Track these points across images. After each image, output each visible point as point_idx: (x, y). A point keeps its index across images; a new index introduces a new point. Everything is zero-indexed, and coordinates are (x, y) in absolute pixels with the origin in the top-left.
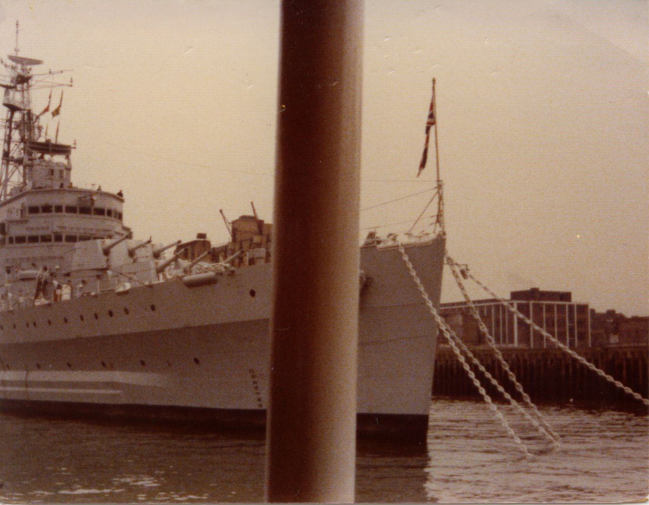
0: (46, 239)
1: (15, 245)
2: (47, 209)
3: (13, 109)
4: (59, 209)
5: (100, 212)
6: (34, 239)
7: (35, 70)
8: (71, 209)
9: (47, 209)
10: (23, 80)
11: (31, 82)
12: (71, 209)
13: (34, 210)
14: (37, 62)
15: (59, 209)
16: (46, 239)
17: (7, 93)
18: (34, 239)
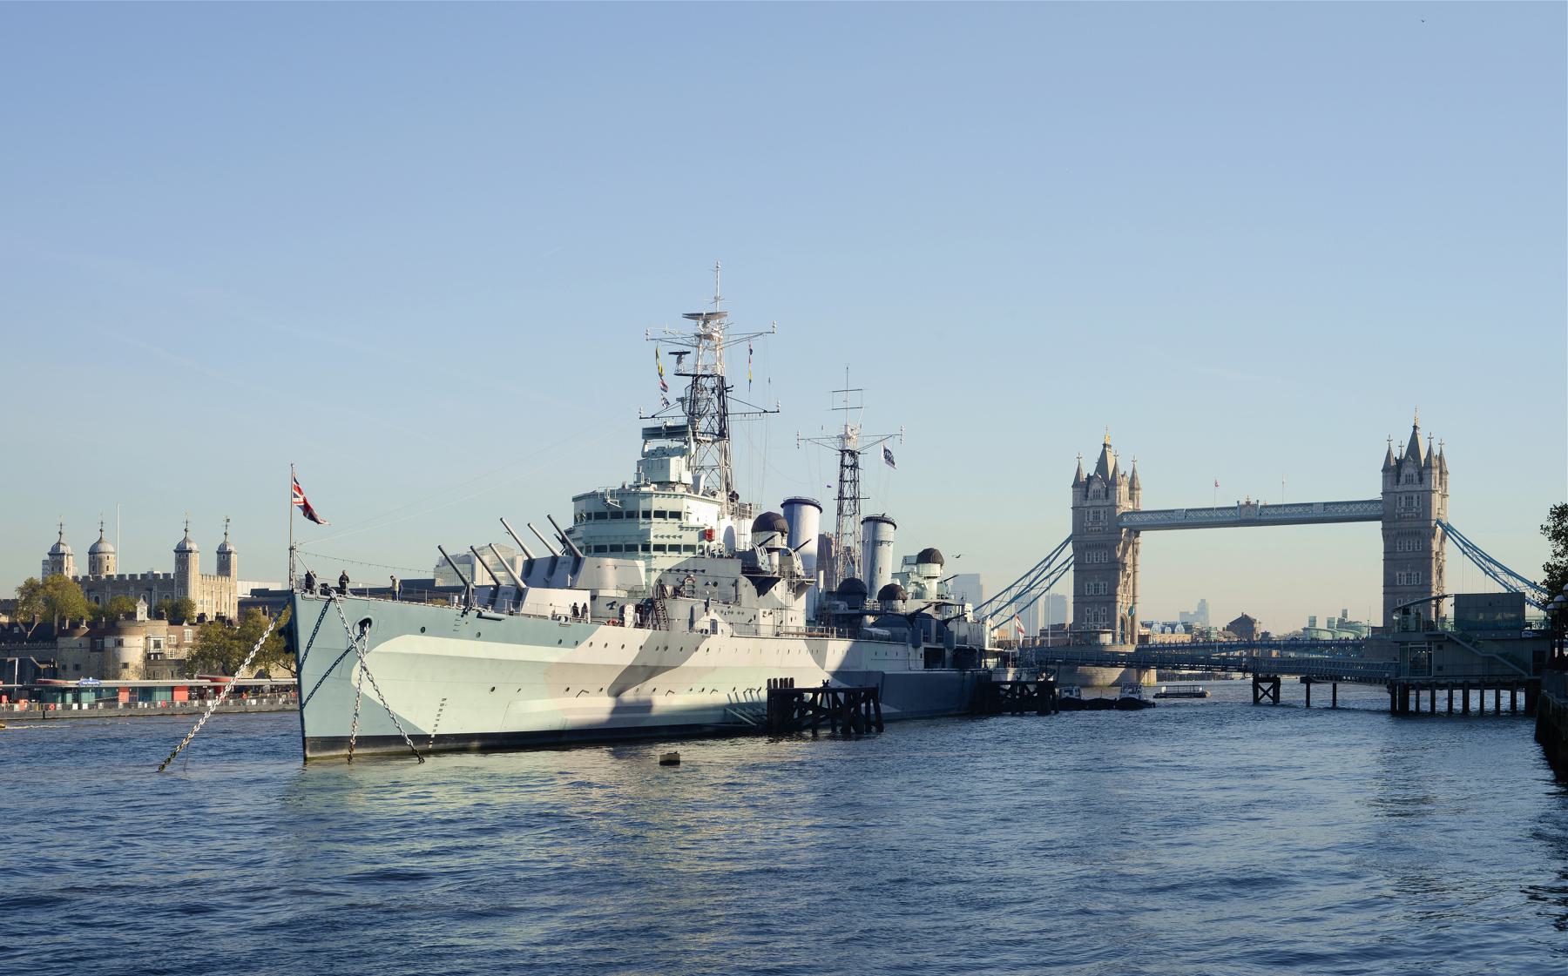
3: (696, 377)
5: (632, 515)
8: (600, 516)
12: (600, 516)
17: (679, 361)
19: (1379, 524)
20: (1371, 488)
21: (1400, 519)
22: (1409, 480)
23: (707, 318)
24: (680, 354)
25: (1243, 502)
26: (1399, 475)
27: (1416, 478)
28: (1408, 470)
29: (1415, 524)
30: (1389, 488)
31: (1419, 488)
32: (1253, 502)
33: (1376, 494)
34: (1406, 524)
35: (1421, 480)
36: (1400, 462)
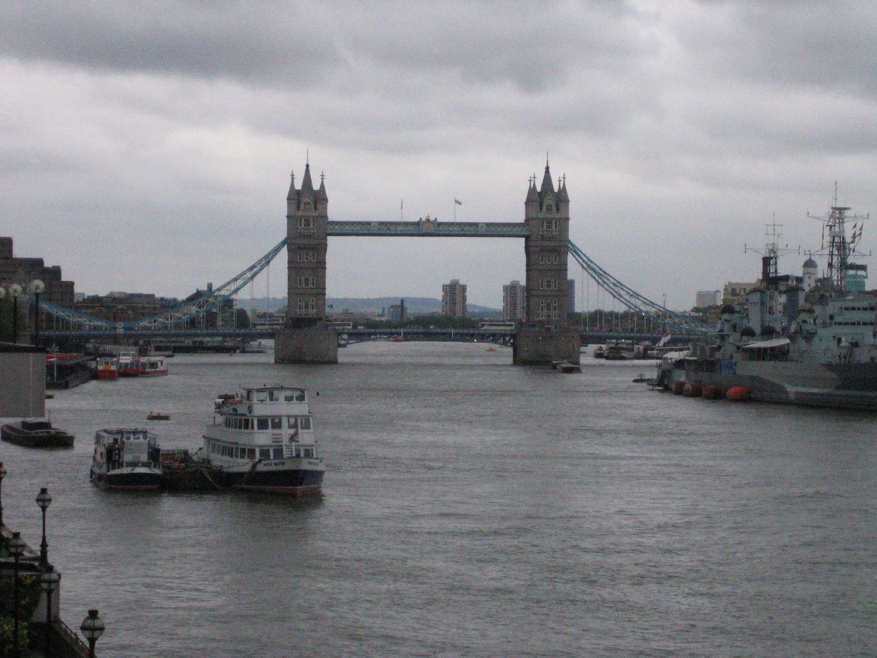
0: (853, 324)
1: (837, 326)
2: (853, 309)
4: (859, 309)
6: (846, 324)
7: (847, 213)
8: (865, 309)
9: (853, 309)
10: (841, 220)
11: (845, 220)
12: (865, 309)
13: (847, 309)
14: (845, 209)
15: (859, 309)
16: (853, 324)
18: (846, 324)
19: (521, 242)
20: (518, 214)
21: (543, 238)
22: (549, 209)
23: (841, 210)
24: (831, 226)
25: (424, 219)
26: (541, 205)
27: (554, 208)
28: (549, 201)
29: (552, 244)
30: (534, 214)
31: (556, 216)
32: (432, 219)
33: (521, 218)
34: (546, 243)
35: (558, 209)
36: (539, 193)
